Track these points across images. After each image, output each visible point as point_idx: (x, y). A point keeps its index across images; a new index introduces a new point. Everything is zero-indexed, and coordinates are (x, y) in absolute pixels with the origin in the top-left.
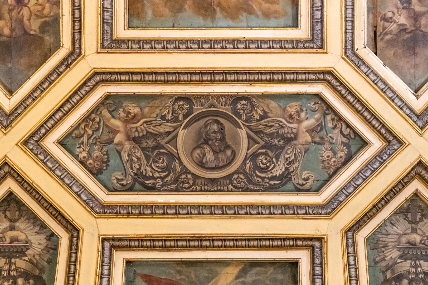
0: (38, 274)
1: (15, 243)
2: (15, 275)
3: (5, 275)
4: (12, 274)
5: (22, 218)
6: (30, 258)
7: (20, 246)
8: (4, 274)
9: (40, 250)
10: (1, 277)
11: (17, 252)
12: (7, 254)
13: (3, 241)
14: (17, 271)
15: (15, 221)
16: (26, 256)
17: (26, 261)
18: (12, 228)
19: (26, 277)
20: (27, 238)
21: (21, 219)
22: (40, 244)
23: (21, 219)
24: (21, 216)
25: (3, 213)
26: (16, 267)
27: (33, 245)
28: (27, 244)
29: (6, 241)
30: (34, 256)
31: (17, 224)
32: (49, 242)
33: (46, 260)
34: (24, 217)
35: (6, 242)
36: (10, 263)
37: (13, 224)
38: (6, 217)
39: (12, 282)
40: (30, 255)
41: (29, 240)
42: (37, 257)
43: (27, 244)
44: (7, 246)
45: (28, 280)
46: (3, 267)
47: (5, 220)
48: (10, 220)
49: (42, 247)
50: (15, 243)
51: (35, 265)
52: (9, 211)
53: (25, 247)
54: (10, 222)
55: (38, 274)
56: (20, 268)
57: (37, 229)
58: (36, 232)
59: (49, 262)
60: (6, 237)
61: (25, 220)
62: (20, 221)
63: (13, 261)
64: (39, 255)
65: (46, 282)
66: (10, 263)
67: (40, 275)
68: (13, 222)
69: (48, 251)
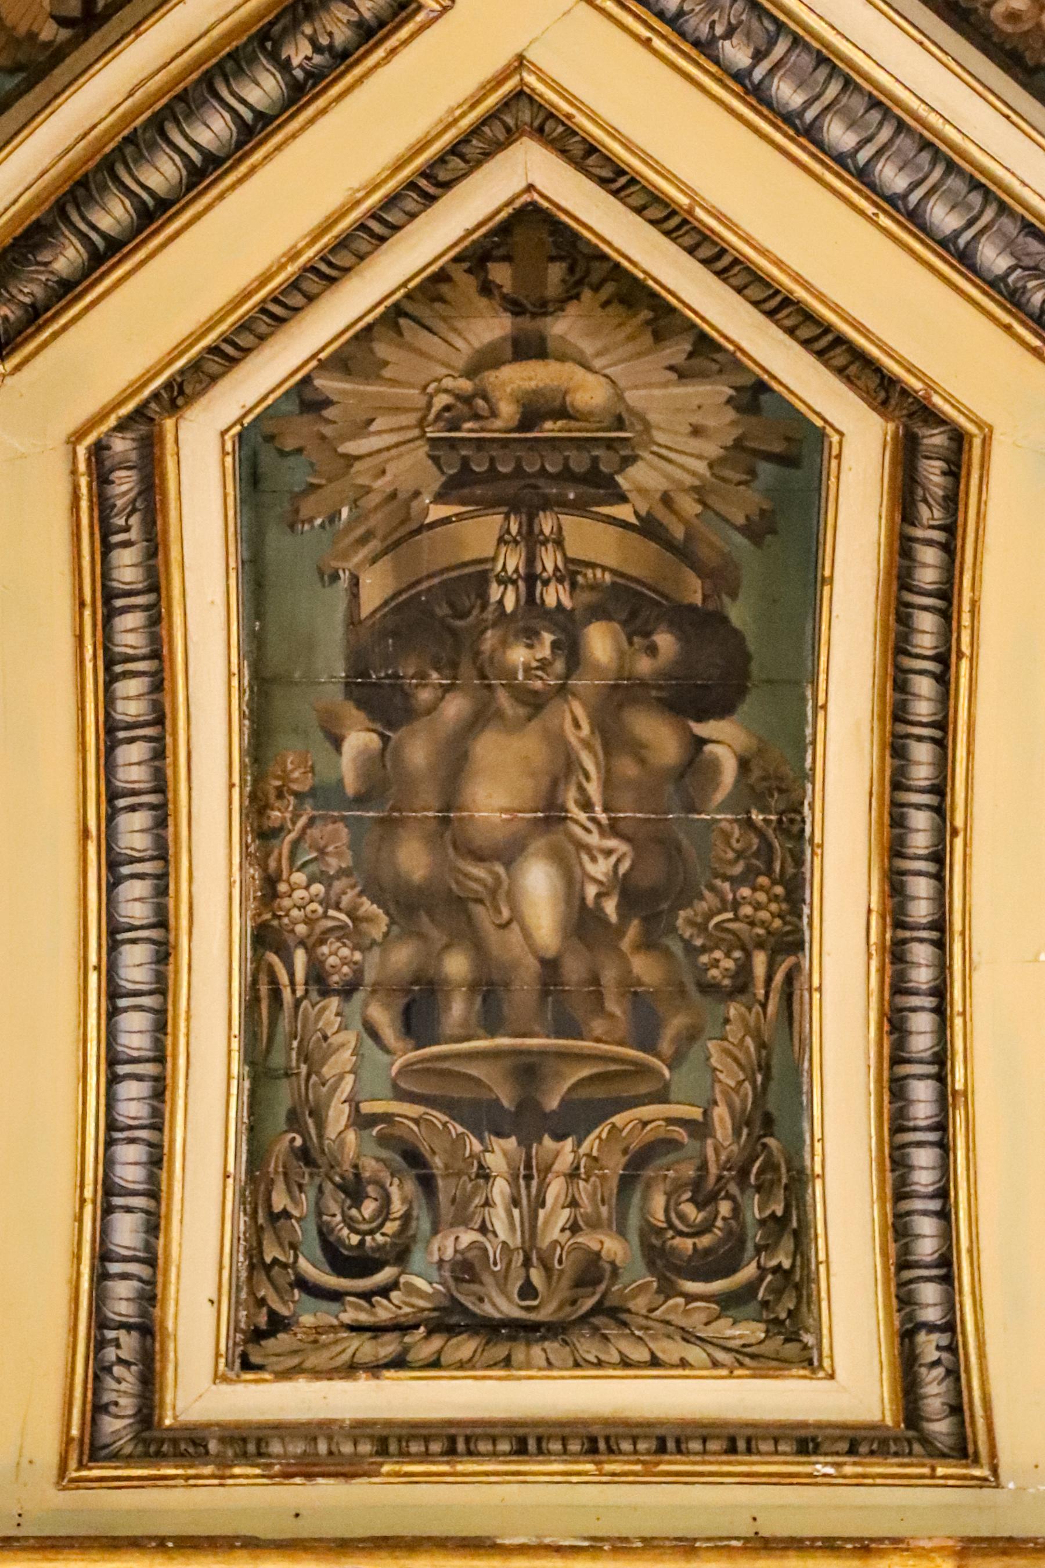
0: (698, 599)
1: (548, 425)
2: (567, 603)
3: (509, 605)
4: (551, 601)
5: (587, 294)
6: (643, 513)
7: (581, 444)
8: (501, 602)
9: (701, 467)
10: (489, 615)
11: (567, 476)
12: (511, 489)
13: (477, 417)
14: (574, 585)
15: (544, 308)
16: (622, 498)
17: (624, 525)
18: (528, 348)
19: (633, 615)
20: (620, 397)
21: (577, 297)
22: (697, 431)
23: (577, 297)
24: (580, 283)
25: (469, 271)
26: (567, 560)
27: (659, 437)
28: (619, 436)
29: (494, 414)
30: (666, 500)
31: (561, 327)
32: (754, 420)
33: (741, 520)
34: (596, 288)
35: (498, 424)
36: (532, 540)
37: (526, 323)
38: (487, 289)
39: (555, 645)
40: (642, 491)
41: (629, 409)
42: (689, 506)
43: (619, 436)
44: (505, 443)
45: (647, 634)
46: (494, 559)
47: (482, 302)
48: (515, 307)
49: (713, 450)
50: (550, 428)
51: (682, 552)
52: (507, 258)
53: (609, 447)
54: (516, 314)
55: (698, 599)
56: (593, 565)
57: (677, 351)
58: (671, 368)
59: (759, 530)
60: (495, 395)
61: (605, 305)
62: (572, 309)
63: (547, 524)
64: (700, 493)
65: (752, 646)
66: (531, 540)
67: (711, 606)
68: (534, 315)
69: (752, 472)
